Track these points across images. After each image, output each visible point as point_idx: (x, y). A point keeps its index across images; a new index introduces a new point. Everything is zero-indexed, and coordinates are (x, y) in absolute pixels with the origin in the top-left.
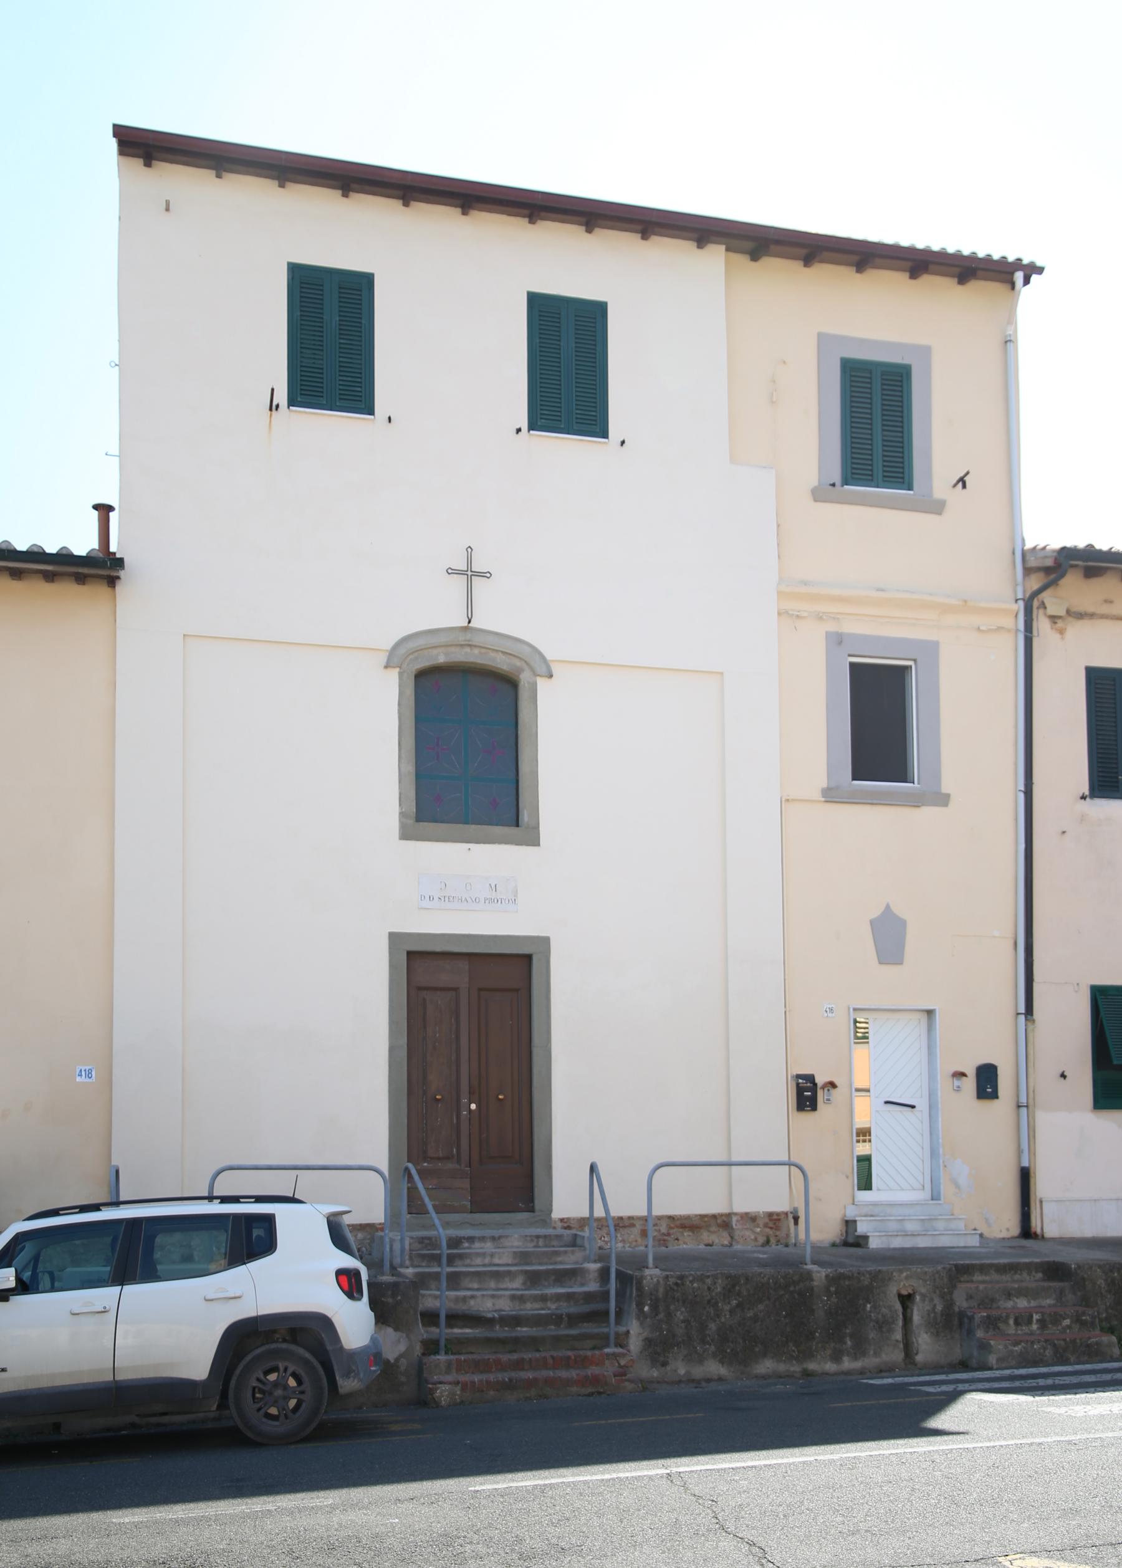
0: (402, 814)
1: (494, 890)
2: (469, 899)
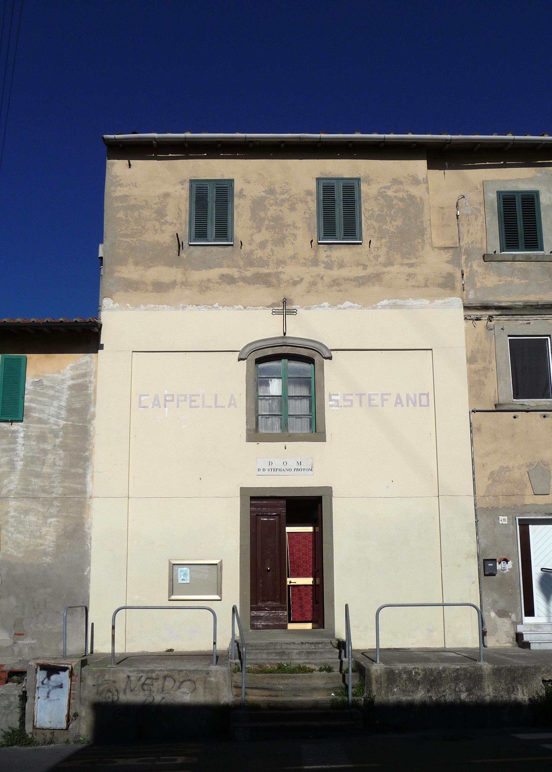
0: (248, 430)
1: (300, 464)
2: (285, 470)
